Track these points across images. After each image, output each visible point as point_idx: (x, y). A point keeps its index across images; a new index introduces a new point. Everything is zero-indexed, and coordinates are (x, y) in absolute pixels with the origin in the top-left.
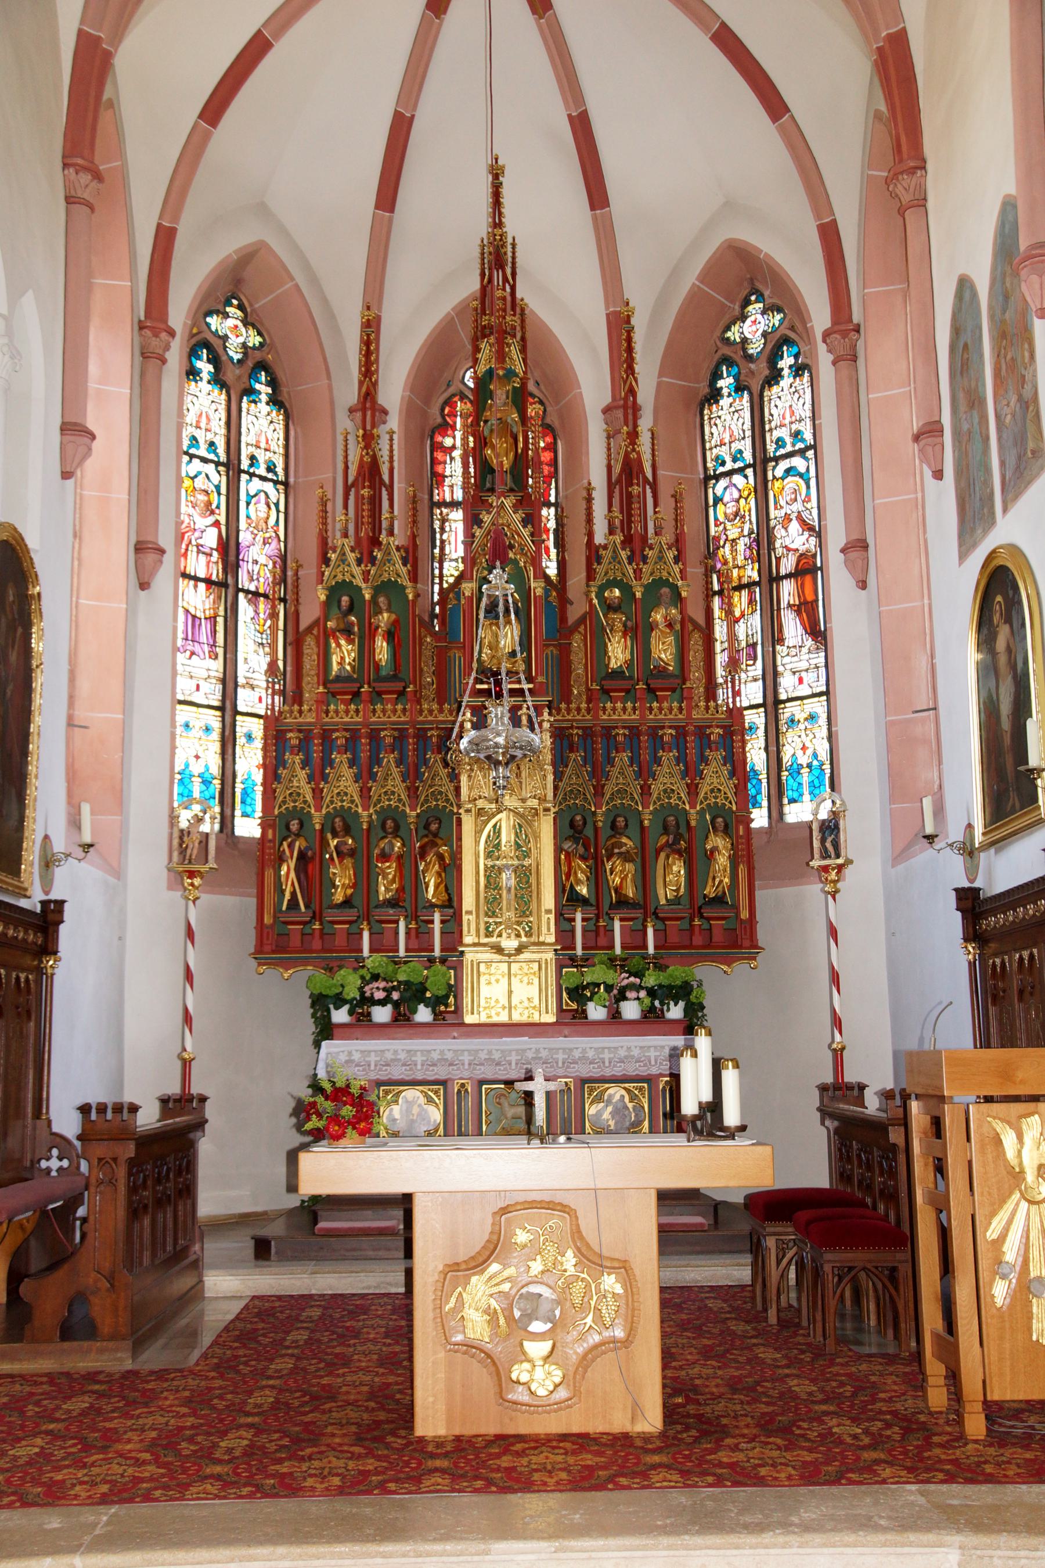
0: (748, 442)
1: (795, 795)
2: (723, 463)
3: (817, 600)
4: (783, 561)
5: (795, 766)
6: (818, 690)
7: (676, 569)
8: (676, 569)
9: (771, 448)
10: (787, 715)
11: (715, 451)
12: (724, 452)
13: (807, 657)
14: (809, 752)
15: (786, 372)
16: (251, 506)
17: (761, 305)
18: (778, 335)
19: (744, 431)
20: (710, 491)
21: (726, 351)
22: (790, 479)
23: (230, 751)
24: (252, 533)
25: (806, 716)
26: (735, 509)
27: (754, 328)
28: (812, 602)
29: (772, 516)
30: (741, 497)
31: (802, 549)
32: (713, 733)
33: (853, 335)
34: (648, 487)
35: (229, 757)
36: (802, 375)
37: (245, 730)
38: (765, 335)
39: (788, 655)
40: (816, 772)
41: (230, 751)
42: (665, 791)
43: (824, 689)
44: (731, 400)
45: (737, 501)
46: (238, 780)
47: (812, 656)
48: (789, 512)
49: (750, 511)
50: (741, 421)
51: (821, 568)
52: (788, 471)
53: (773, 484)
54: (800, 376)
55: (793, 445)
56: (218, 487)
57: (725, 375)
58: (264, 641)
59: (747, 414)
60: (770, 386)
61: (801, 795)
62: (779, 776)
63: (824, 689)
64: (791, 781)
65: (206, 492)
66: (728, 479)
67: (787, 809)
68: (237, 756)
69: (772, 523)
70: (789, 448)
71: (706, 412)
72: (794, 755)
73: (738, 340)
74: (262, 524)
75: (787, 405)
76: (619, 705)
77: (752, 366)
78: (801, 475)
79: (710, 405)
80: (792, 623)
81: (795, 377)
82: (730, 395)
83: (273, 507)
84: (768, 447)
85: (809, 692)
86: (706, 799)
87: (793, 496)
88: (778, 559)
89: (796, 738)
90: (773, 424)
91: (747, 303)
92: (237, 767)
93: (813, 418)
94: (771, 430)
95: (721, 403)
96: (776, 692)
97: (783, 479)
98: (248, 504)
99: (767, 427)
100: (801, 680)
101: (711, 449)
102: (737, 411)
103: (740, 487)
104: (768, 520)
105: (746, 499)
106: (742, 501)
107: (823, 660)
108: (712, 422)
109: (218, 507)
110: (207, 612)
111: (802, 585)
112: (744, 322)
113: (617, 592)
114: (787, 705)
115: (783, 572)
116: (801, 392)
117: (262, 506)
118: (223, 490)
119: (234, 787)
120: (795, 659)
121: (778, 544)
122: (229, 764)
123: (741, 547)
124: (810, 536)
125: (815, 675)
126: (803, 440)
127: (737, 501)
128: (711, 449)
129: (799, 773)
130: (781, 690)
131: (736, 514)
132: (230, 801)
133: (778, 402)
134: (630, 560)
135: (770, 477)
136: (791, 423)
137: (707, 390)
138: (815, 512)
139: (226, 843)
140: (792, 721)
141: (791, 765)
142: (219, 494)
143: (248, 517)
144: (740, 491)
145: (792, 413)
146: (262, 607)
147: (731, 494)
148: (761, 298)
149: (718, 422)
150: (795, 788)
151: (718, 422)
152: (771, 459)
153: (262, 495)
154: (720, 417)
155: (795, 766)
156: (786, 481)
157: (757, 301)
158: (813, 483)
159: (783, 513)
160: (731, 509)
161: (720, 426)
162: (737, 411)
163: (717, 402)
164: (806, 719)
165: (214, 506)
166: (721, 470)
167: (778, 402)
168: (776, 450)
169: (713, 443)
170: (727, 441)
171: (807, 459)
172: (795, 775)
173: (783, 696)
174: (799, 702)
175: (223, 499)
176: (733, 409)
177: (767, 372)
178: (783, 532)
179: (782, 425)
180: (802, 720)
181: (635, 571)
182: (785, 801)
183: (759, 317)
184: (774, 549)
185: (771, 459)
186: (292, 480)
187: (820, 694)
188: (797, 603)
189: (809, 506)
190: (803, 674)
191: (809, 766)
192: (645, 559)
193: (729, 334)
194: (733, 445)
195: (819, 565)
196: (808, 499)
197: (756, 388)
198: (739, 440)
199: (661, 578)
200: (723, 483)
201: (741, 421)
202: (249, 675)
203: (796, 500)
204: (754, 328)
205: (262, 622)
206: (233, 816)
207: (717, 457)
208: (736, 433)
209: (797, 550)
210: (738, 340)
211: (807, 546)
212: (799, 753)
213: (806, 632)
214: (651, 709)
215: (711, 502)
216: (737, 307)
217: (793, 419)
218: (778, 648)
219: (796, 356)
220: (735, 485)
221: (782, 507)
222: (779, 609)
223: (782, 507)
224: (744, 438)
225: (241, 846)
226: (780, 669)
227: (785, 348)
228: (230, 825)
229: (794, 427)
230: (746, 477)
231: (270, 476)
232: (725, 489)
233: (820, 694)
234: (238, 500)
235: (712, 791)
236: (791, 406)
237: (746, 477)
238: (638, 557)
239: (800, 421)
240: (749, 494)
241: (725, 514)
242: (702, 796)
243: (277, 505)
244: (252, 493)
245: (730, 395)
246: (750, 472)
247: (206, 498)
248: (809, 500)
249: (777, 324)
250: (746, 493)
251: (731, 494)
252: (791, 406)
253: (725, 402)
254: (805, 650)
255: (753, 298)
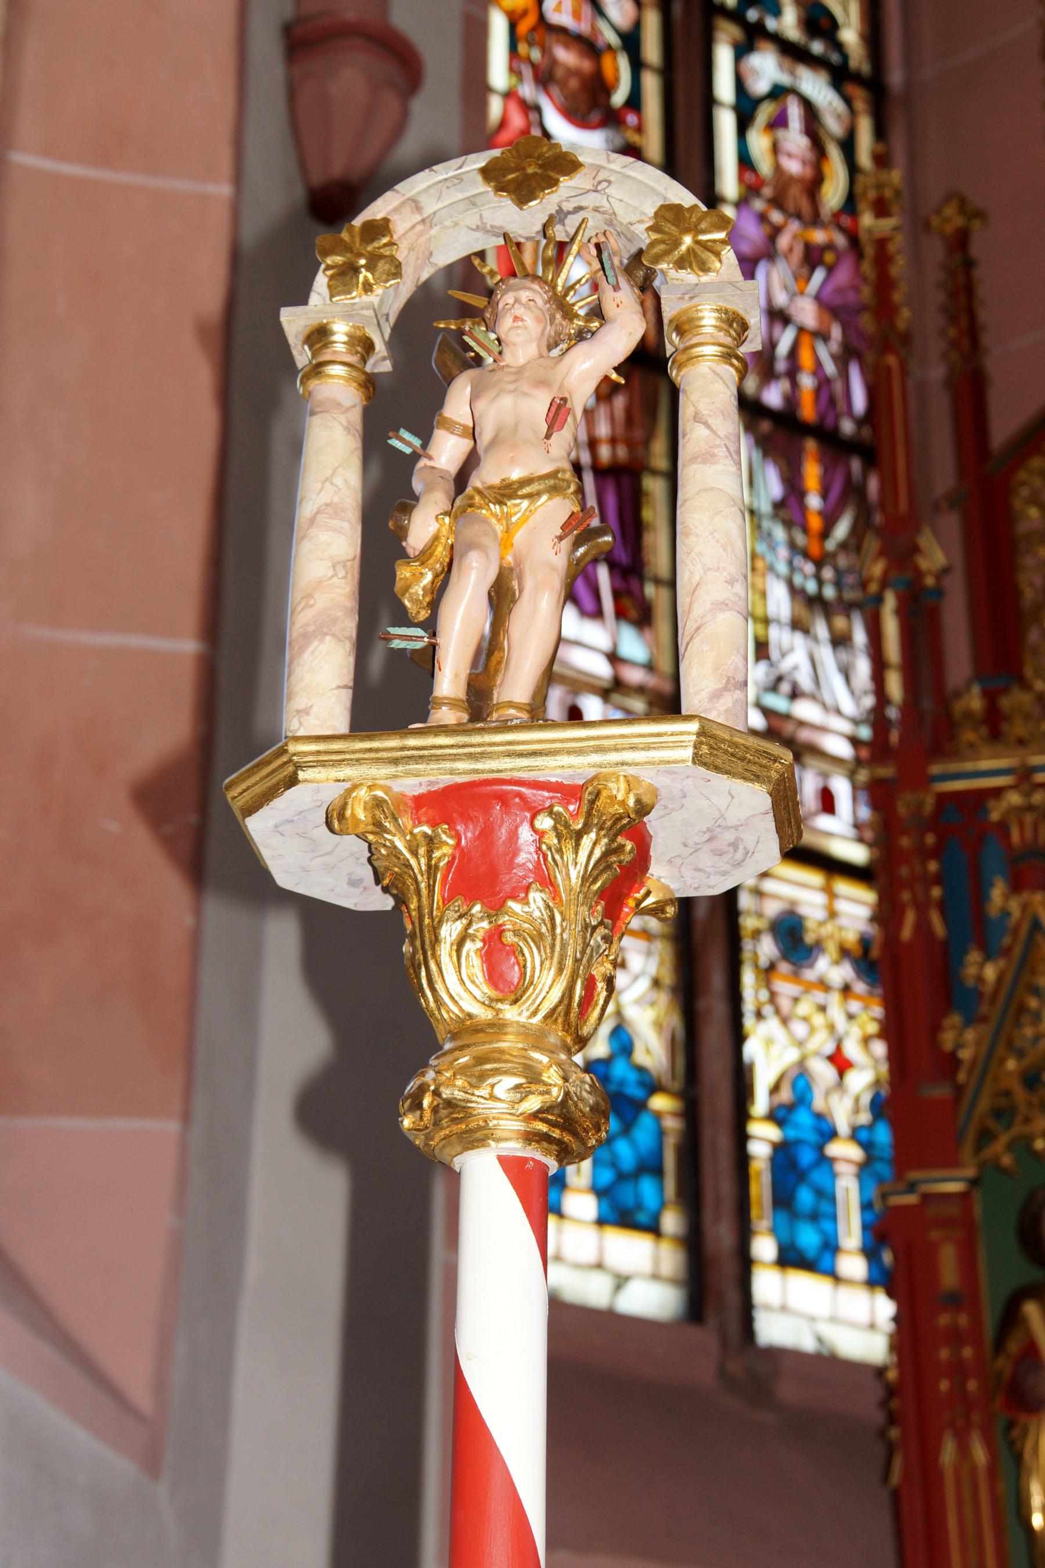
16: (759, 142)
23: (717, 981)
24: (763, 218)
35: (715, 1006)
37: (772, 909)
41: (717, 981)
46: (760, 1104)
56: (631, 41)
58: (829, 592)
65: (588, 46)
68: (749, 1006)
74: (796, 196)
83: (835, 154)
92: (752, 1049)
98: (743, 125)
109: (634, 102)
110: (605, 452)
117: (795, 139)
118: (652, 50)
119: (742, 1138)
122: (714, 1034)
132: (727, 1187)
139: (722, 1373)
142: (637, 65)
143: (745, 162)
146: (812, 473)
153: (795, 112)
165: (619, 98)
175: (651, 84)
186: (895, 77)
202: (778, 703)
205: (815, 523)
206: (746, 1263)
225: (787, 1391)
228: (732, 1297)
231: (817, 47)
234: (709, 101)
243: (848, 146)
244: (760, 86)
247: (587, 65)
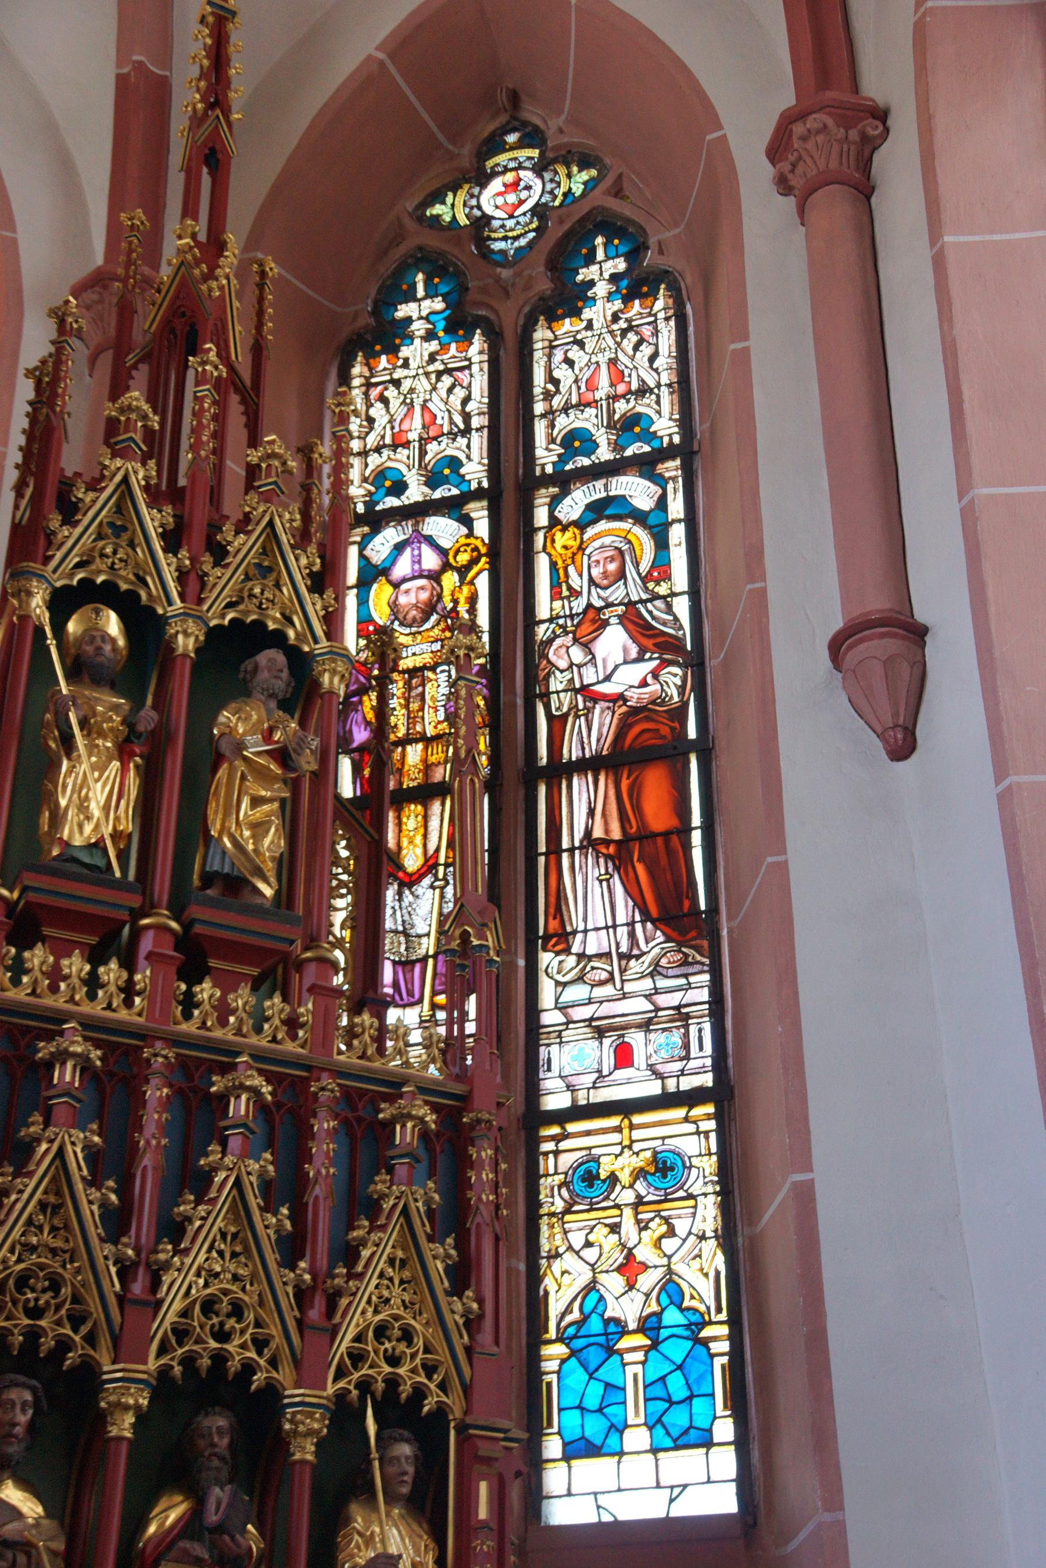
0: (479, 442)
1: (594, 1428)
2: (399, 488)
3: (686, 830)
4: (573, 728)
5: (595, 1325)
6: (687, 1083)
7: (314, 606)
8: (314, 606)
9: (546, 456)
10: (566, 1160)
11: (374, 460)
12: (401, 461)
13: (647, 984)
14: (647, 1281)
15: (601, 289)
17: (535, 153)
18: (584, 208)
19: (467, 417)
20: (353, 552)
21: (432, 241)
22: (603, 525)
25: (637, 1162)
26: (424, 596)
27: (511, 198)
28: (667, 834)
29: (543, 611)
30: (446, 566)
31: (635, 696)
32: (403, 1117)
33: (874, 130)
34: (234, 399)
36: (654, 295)
38: (539, 211)
39: (580, 979)
40: (677, 1350)
42: (209, 1306)
43: (707, 1080)
44: (434, 346)
45: (435, 577)
47: (662, 983)
48: (598, 603)
49: (473, 600)
50: (460, 393)
51: (705, 749)
52: (598, 510)
53: (550, 539)
54: (642, 296)
55: (617, 447)
57: (420, 292)
59: (479, 383)
60: (552, 319)
61: (619, 1429)
62: (534, 1360)
63: (707, 1080)
64: (576, 1375)
66: (409, 527)
67: (554, 1478)
69: (542, 632)
70: (604, 454)
71: (356, 370)
72: (591, 1287)
73: (463, 221)
75: (603, 359)
76: (76, 965)
77: (505, 273)
78: (639, 517)
79: (371, 357)
80: (596, 890)
81: (627, 300)
82: (430, 336)
84: (539, 452)
85: (654, 1088)
86: (357, 1358)
87: (612, 567)
88: (557, 724)
89: (600, 1234)
90: (557, 402)
91: (494, 145)
93: (682, 386)
94: (550, 414)
95: (405, 352)
96: (533, 1091)
97: (581, 525)
99: (539, 408)
100: (624, 1057)
101: (364, 454)
102: (449, 371)
103: (446, 544)
104: (531, 621)
105: (463, 571)
106: (450, 580)
107: (704, 995)
108: (374, 393)
111: (636, 792)
112: (483, 185)
113: (113, 624)
114: (572, 1127)
115: (571, 751)
116: (647, 331)
120: (608, 990)
121: (557, 683)
123: (438, 687)
124: (665, 663)
125: (676, 1038)
126: (650, 436)
127: (435, 577)
128: (364, 454)
129: (610, 1351)
130: (550, 1083)
131: (429, 609)
133: (575, 353)
134: (172, 540)
135: (541, 517)
136: (616, 398)
137: (366, 320)
138: (682, 607)
140: (590, 1178)
141: (581, 1323)
144: (443, 552)
145: (617, 376)
147: (417, 560)
148: (532, 137)
149: (391, 393)
150: (592, 1401)
151: (391, 393)
152: (546, 480)
154: (397, 383)
155: (595, 1325)
156: (590, 532)
157: (520, 145)
158: (677, 534)
159: (579, 605)
160: (414, 594)
161: (395, 404)
162: (449, 371)
163: (393, 350)
164: (639, 1174)
166: (392, 502)
167: (575, 353)
168: (562, 459)
169: (372, 440)
170: (413, 436)
171: (660, 481)
172: (594, 1356)
173: (555, 1101)
174: (614, 1121)
176: (438, 366)
177: (544, 285)
178: (577, 655)
179: (582, 405)
180: (625, 1177)
181: (182, 577)
182: (553, 1447)
183: (527, 176)
184: (546, 696)
185: (546, 480)
187: (691, 1098)
188: (616, 834)
189: (663, 589)
190: (636, 1039)
191: (650, 1325)
192: (220, 553)
193: (438, 209)
194: (432, 448)
195: (692, 733)
196: (661, 570)
197: (509, 316)
198: (453, 436)
199: (260, 624)
200: (390, 536)
201: (460, 393)
203: (621, 575)
204: (511, 198)
207: (381, 474)
208: (442, 419)
209: (621, 698)
210: (463, 221)
211: (654, 688)
212: (613, 1283)
213: (646, 917)
214: (189, 1003)
215: (352, 576)
216: (466, 152)
217: (621, 388)
218: (546, 958)
219: (633, 256)
220: (430, 541)
221: (575, 593)
222: (555, 849)
223: (575, 593)
224: (466, 431)
226: (550, 1018)
227: (599, 240)
229: (621, 407)
230: (467, 521)
232: (399, 548)
233: (691, 1098)
235: (381, 1332)
236: (613, 362)
237: (467, 521)
238: (198, 534)
239: (643, 391)
240: (474, 561)
241: (394, 606)
242: (345, 1343)
245: (430, 336)
246: (480, 515)
248: (666, 576)
249: (578, 189)
250: (463, 558)
251: (417, 560)
252: (613, 362)
253: (415, 351)
254: (635, 967)
255: (512, 138)
